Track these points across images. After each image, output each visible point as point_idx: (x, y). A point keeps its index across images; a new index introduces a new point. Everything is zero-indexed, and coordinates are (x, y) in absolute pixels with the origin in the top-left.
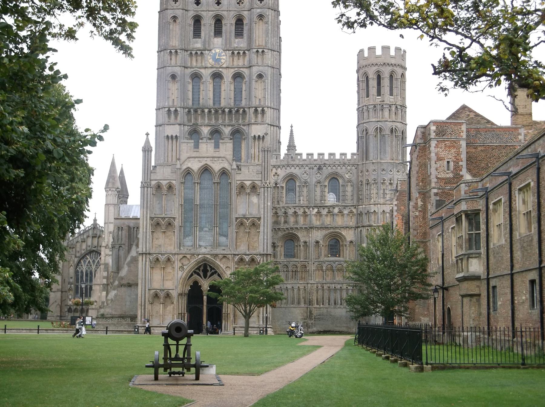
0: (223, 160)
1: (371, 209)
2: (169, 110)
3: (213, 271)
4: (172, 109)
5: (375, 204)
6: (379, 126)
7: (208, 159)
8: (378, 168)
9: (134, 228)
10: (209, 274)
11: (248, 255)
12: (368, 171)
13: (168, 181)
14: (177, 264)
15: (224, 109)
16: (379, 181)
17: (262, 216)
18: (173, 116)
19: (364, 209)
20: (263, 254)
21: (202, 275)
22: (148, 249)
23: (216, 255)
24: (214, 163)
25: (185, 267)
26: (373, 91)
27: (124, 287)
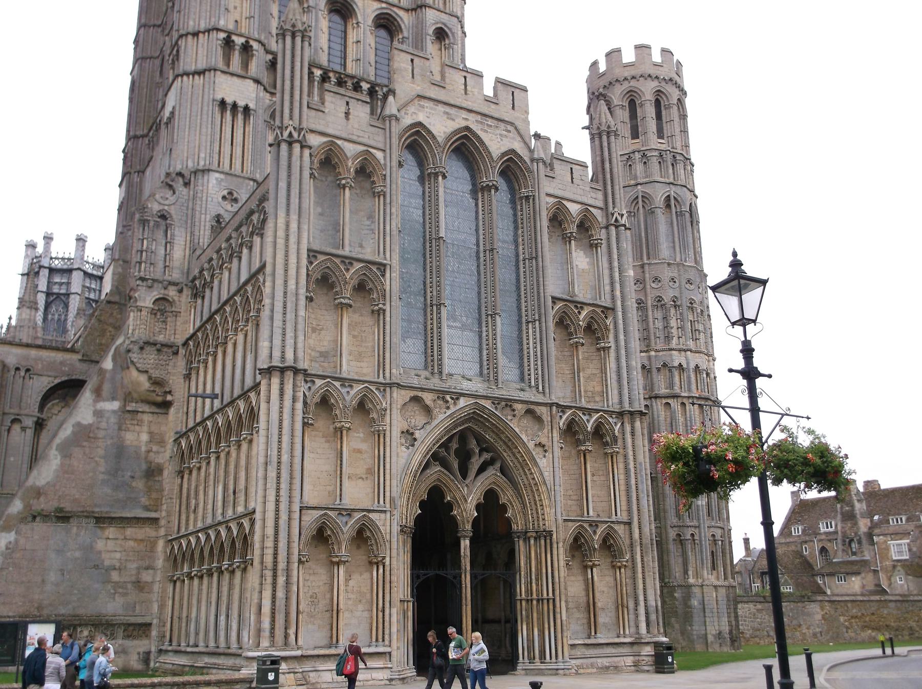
0: (509, 131)
1: (672, 361)
2: (228, 43)
3: (486, 456)
4: (239, 41)
5: (680, 350)
6: (672, 193)
7: (472, 117)
8: (679, 275)
9: (17, 369)
10: (476, 462)
11: (589, 412)
12: (656, 279)
13: (365, 148)
14: (395, 423)
15: (358, 83)
16: (684, 303)
17: (619, 303)
18: (236, 58)
19: (653, 360)
20: (631, 413)
21: (455, 465)
22: (300, 354)
23: (508, 403)
24: (487, 132)
25: (417, 434)
26: (652, 125)
27: (44, 522)
